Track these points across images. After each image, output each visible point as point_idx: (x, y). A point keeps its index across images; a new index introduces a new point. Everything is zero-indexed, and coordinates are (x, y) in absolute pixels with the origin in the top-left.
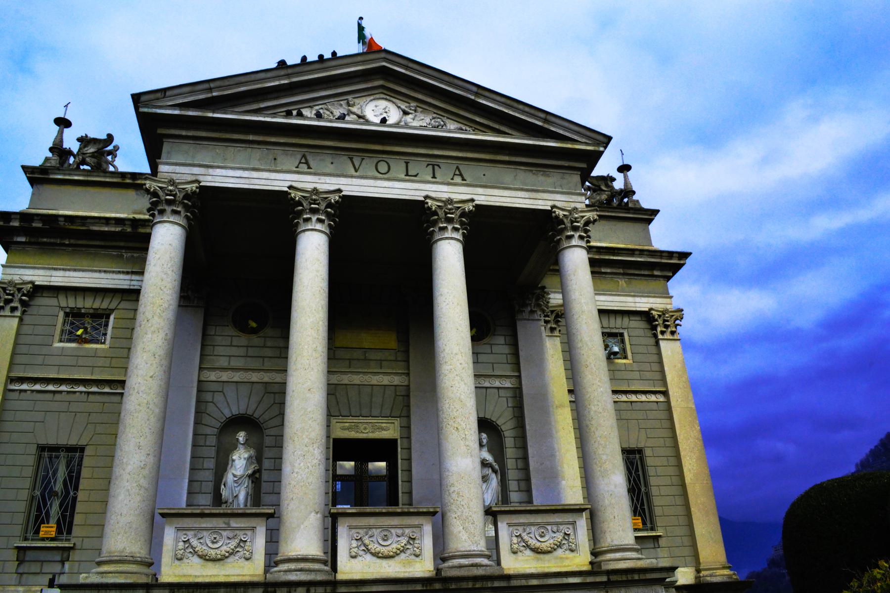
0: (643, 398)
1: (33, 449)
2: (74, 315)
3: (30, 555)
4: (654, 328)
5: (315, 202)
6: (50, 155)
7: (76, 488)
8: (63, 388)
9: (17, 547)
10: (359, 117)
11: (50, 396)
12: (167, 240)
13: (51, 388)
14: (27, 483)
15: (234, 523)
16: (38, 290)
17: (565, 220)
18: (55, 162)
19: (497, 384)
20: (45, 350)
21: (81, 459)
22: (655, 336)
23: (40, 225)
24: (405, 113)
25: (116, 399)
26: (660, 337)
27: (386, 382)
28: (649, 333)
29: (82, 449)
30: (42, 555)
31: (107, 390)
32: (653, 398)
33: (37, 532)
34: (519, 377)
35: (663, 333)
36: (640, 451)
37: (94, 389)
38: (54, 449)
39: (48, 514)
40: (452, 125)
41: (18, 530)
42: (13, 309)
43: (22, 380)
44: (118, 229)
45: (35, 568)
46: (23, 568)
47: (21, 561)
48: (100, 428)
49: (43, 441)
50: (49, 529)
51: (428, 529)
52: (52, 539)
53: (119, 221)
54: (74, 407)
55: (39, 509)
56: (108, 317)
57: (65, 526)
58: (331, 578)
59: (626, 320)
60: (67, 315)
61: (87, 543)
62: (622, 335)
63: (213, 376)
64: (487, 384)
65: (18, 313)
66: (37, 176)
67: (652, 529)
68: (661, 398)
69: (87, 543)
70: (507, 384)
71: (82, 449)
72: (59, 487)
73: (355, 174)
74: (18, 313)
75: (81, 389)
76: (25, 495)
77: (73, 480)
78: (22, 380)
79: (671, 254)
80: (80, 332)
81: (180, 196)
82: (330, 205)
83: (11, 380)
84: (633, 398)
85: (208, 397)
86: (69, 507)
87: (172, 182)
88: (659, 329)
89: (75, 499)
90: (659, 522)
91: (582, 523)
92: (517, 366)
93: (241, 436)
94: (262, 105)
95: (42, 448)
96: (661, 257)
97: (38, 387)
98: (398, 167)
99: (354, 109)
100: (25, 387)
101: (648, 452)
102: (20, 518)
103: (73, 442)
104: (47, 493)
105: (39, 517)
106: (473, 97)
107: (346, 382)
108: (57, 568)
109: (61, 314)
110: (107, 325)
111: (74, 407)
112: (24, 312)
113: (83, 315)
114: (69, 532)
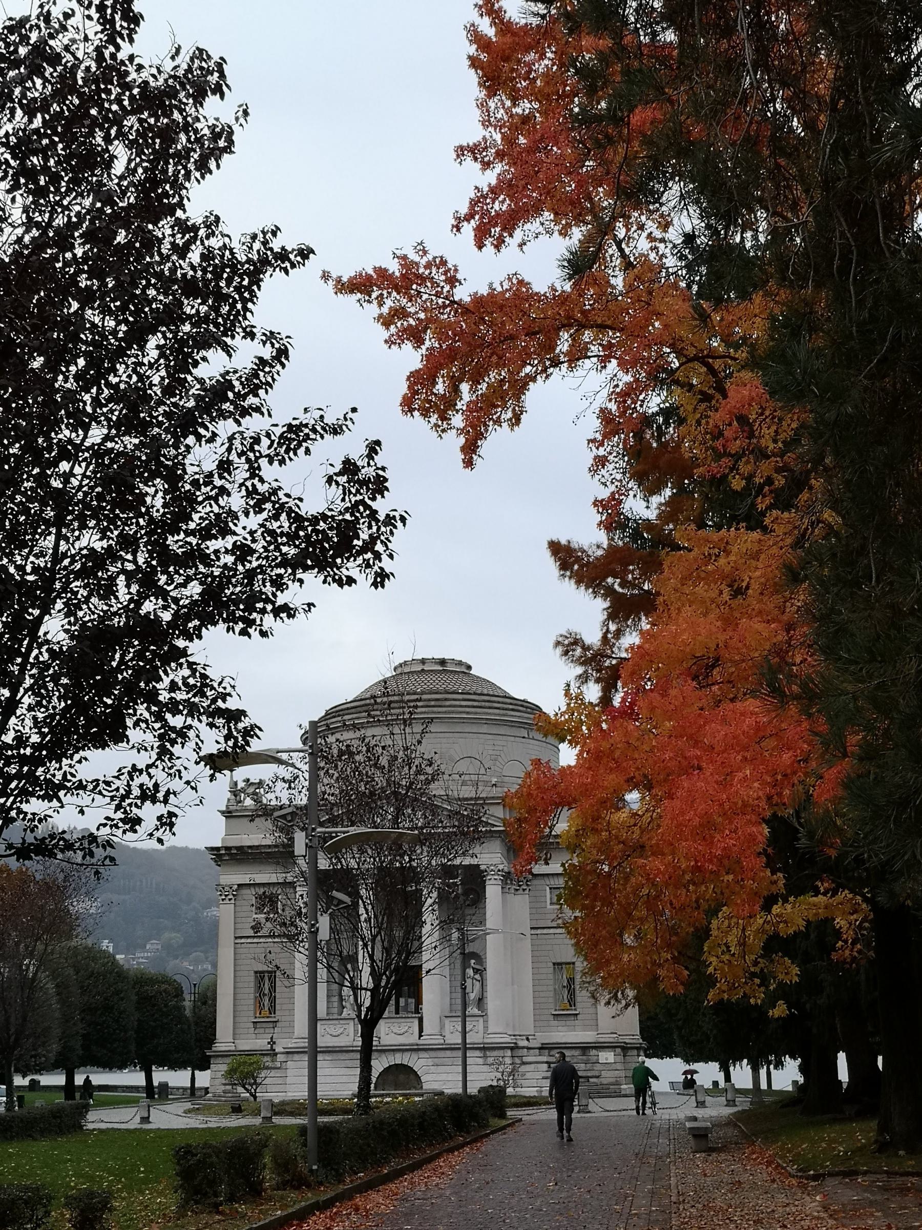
3: (258, 1025)
6: (229, 795)
16: (240, 886)
18: (233, 802)
30: (264, 1025)
43: (241, 937)
45: (262, 1031)
47: (255, 1028)
51: (416, 1022)
57: (273, 1009)
61: (283, 1019)
66: (228, 814)
78: (241, 937)
83: (236, 938)
95: (256, 972)
100: (243, 941)
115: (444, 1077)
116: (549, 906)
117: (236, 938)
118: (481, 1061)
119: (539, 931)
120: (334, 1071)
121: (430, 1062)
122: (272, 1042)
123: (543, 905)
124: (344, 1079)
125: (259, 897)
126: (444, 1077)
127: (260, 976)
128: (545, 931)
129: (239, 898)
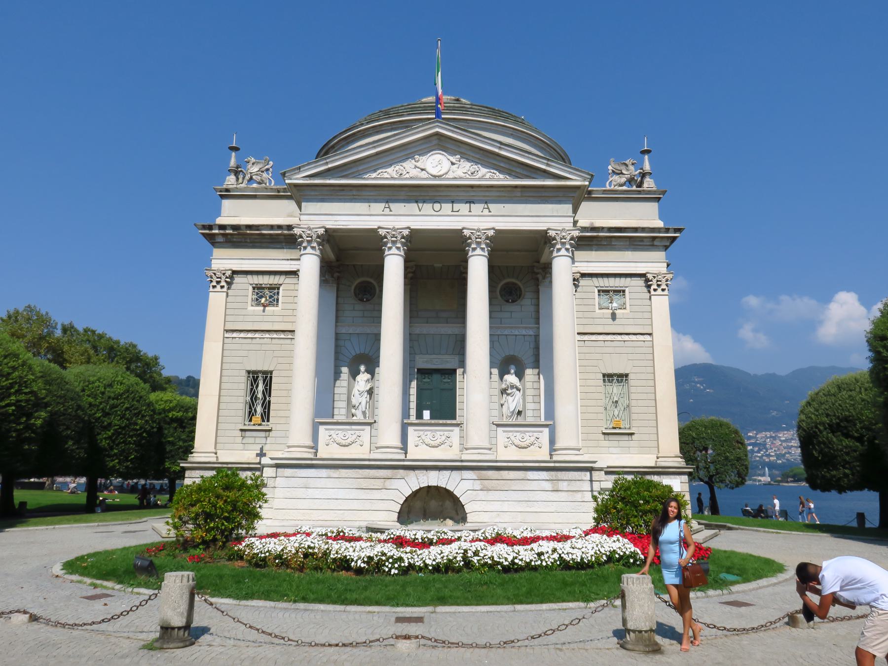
0: (633, 338)
1: (244, 373)
2: (258, 288)
3: (248, 434)
4: (649, 287)
5: (393, 236)
7: (270, 396)
8: (257, 335)
9: (242, 430)
10: (422, 170)
11: (249, 341)
12: (309, 264)
13: (250, 335)
14: (243, 393)
15: (354, 427)
17: (557, 238)
19: (524, 332)
20: (243, 312)
21: (271, 377)
22: (649, 292)
23: (231, 232)
24: (453, 164)
25: (289, 341)
26: (653, 292)
27: (450, 332)
28: (645, 290)
29: (271, 372)
31: (282, 336)
32: (641, 338)
33: (250, 420)
34: (538, 328)
35: (655, 290)
36: (627, 375)
37: (275, 336)
38: (254, 372)
39: (255, 410)
40: (483, 171)
41: (241, 419)
42: (222, 287)
44: (280, 232)
45: (251, 440)
46: (246, 441)
47: (243, 437)
48: (281, 360)
49: (249, 369)
50: (257, 418)
52: (260, 425)
53: (280, 227)
54: (264, 347)
55: (250, 408)
56: (278, 289)
57: (266, 416)
58: (402, 457)
59: (628, 279)
60: (254, 288)
62: (624, 291)
63: (343, 331)
64: (517, 333)
65: (225, 289)
67: (629, 428)
68: (648, 338)
69: (279, 427)
70: (531, 333)
71: (271, 372)
72: (260, 395)
73: (419, 213)
74: (225, 289)
75: (267, 336)
76: (242, 400)
77: (268, 391)
79: (667, 230)
80: (263, 300)
81: (314, 236)
82: (403, 237)
84: (626, 338)
85: (341, 343)
86: (267, 406)
87: (310, 229)
88: (652, 287)
89: (269, 402)
90: (634, 423)
91: (546, 431)
92: (537, 320)
93: (362, 368)
94: (360, 168)
95: (249, 372)
96: (660, 232)
97: (242, 335)
98: (447, 207)
99: (418, 164)
100: (235, 335)
101: (631, 377)
102: (241, 413)
103: (265, 369)
104: (254, 397)
105: (251, 414)
106: (497, 150)
107: (425, 332)
108: (263, 440)
109: (251, 288)
110: (278, 293)
111: (264, 347)
112: (229, 288)
113: (263, 288)
114: (268, 421)
115: (497, 506)
116: (598, 311)
117: (227, 331)
118: (548, 486)
119: (586, 338)
120: (342, 494)
121: (478, 485)
122: (261, 454)
123: (591, 308)
124: (355, 505)
125: (258, 288)
126: (497, 506)
127: (254, 376)
128: (594, 337)
129: (233, 286)
